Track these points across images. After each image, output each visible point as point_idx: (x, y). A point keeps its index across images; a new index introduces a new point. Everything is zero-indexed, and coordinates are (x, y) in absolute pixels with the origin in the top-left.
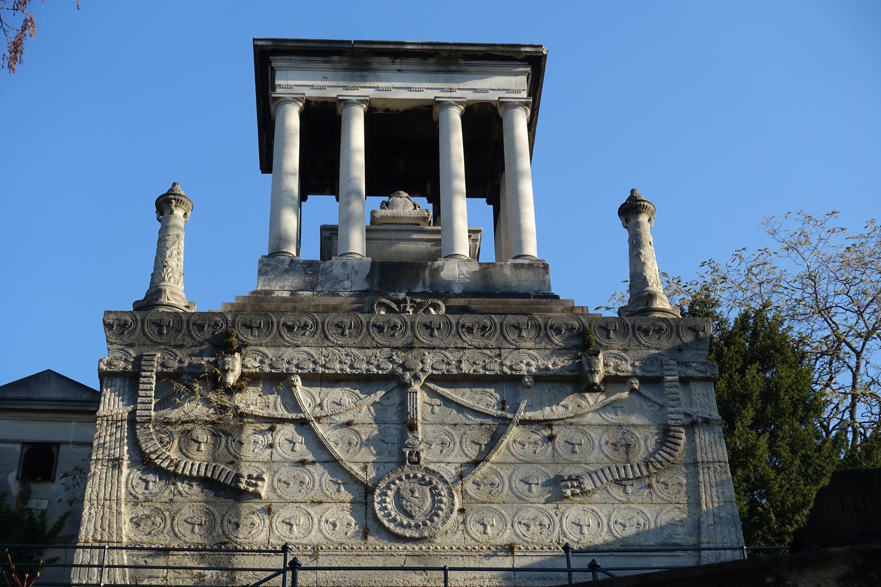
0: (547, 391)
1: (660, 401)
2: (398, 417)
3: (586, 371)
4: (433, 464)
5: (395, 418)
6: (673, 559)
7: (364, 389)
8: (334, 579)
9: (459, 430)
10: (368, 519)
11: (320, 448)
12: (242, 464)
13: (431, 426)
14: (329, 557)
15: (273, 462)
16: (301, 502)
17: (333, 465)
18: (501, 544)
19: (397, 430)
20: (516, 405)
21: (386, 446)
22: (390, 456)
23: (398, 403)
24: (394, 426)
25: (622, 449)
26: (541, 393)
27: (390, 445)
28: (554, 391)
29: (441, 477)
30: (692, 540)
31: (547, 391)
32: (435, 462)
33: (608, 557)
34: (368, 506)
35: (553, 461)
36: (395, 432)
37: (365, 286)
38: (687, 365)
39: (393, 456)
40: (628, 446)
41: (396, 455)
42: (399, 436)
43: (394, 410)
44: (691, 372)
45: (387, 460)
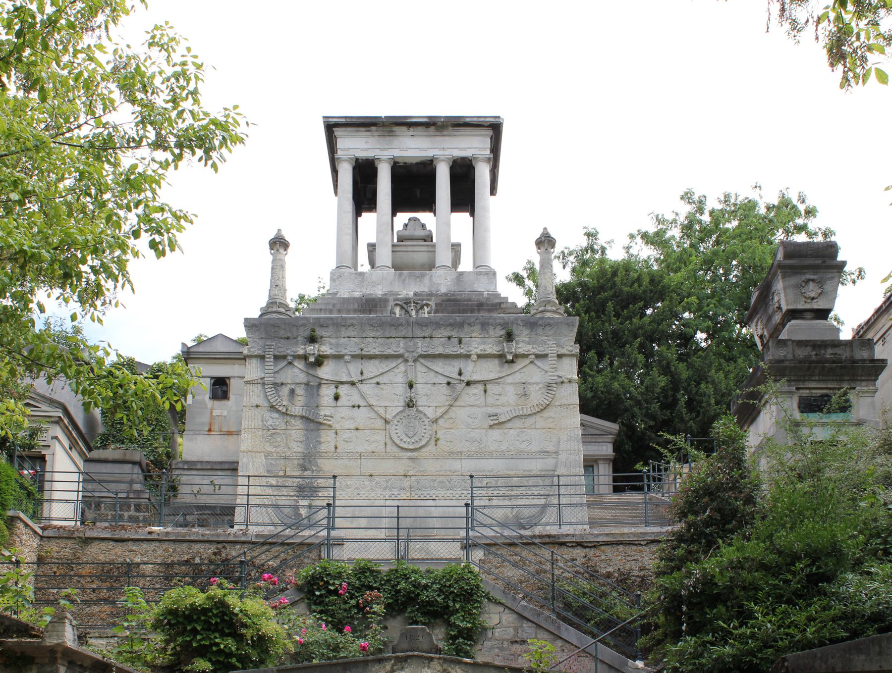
17: (369, 408)
29: (425, 415)
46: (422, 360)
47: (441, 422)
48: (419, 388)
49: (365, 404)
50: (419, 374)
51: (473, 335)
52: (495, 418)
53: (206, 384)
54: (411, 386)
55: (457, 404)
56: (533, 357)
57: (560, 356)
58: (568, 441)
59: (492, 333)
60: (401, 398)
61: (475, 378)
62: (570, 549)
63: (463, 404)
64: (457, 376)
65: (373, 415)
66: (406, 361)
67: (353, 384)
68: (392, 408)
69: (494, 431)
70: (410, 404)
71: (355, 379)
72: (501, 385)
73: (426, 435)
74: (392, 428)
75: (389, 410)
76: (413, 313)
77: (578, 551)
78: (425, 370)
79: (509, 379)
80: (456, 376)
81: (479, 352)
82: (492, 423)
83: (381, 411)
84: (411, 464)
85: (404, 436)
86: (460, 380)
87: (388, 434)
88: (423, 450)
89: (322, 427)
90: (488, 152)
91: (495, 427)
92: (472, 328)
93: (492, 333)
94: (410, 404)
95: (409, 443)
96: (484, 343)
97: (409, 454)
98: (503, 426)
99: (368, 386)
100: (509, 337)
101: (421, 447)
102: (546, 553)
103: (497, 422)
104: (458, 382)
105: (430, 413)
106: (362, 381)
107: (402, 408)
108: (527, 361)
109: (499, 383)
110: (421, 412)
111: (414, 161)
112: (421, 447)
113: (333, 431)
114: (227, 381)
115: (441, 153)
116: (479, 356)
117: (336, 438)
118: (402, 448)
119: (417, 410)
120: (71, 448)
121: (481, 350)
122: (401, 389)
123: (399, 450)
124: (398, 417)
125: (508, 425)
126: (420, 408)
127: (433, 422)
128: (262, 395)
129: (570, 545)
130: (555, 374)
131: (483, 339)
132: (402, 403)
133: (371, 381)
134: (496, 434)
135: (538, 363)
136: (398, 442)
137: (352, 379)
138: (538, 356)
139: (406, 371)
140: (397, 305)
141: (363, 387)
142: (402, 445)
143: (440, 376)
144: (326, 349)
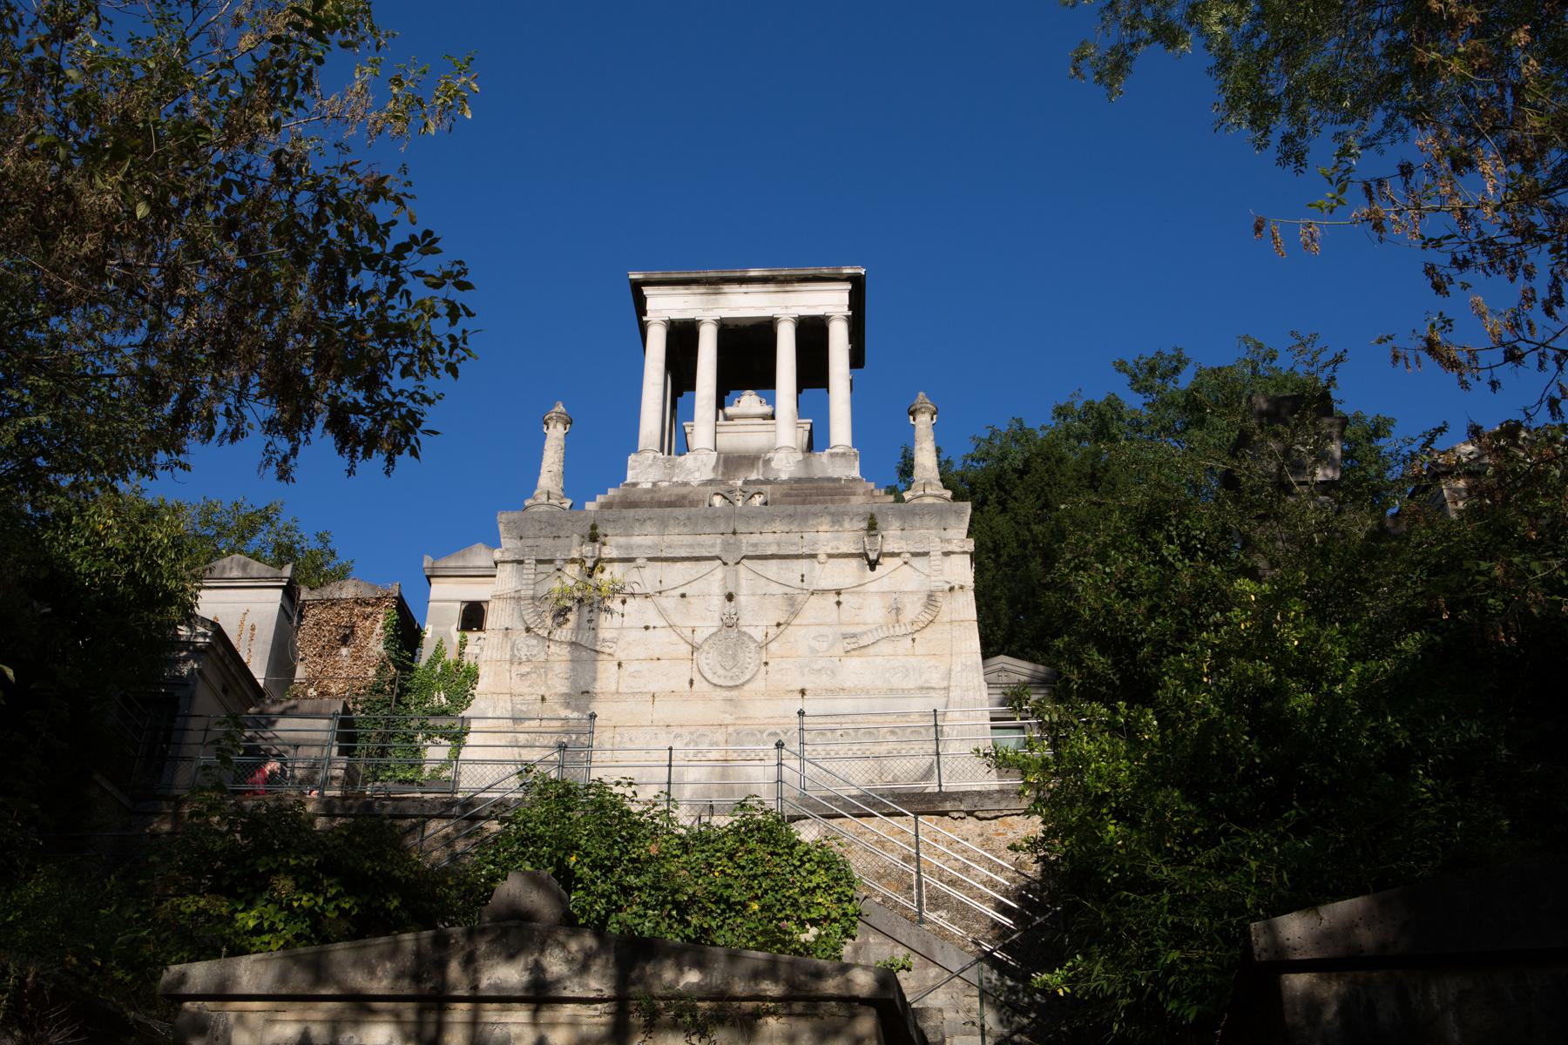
1: (927, 572)
18: (602, 737)
25: (894, 612)
29: (751, 637)
30: (945, 684)
37: (711, 476)
38: (949, 541)
40: (898, 609)
44: (950, 548)
46: (744, 561)
47: (773, 646)
48: (742, 599)
49: (664, 623)
50: (743, 582)
51: (821, 529)
52: (853, 640)
53: (456, 611)
54: (730, 597)
55: (796, 622)
56: (908, 555)
57: (947, 554)
58: (963, 670)
59: (847, 525)
60: (717, 615)
61: (824, 585)
62: (957, 823)
63: (804, 622)
64: (800, 584)
65: (675, 638)
66: (725, 564)
67: (647, 596)
70: (730, 623)
71: (649, 590)
73: (751, 667)
74: (701, 658)
76: (740, 504)
77: (971, 826)
78: (752, 575)
79: (872, 587)
80: (797, 583)
81: (829, 551)
88: (746, 688)
89: (601, 657)
90: (846, 308)
92: (819, 520)
93: (847, 525)
94: (730, 623)
96: (838, 539)
97: (726, 694)
100: (872, 527)
101: (743, 685)
102: (904, 824)
103: (856, 645)
105: (758, 635)
107: (715, 630)
108: (897, 561)
109: (859, 593)
110: (745, 633)
111: (748, 324)
112: (743, 685)
113: (616, 663)
114: (485, 606)
115: (784, 311)
116: (830, 556)
120: (225, 691)
122: (718, 601)
125: (872, 650)
126: (744, 629)
128: (516, 615)
129: (955, 815)
130: (941, 578)
133: (672, 592)
134: (854, 663)
135: (916, 562)
136: (709, 677)
138: (915, 555)
139: (724, 578)
140: (717, 494)
141: (663, 601)
143: (773, 584)
144: (608, 552)
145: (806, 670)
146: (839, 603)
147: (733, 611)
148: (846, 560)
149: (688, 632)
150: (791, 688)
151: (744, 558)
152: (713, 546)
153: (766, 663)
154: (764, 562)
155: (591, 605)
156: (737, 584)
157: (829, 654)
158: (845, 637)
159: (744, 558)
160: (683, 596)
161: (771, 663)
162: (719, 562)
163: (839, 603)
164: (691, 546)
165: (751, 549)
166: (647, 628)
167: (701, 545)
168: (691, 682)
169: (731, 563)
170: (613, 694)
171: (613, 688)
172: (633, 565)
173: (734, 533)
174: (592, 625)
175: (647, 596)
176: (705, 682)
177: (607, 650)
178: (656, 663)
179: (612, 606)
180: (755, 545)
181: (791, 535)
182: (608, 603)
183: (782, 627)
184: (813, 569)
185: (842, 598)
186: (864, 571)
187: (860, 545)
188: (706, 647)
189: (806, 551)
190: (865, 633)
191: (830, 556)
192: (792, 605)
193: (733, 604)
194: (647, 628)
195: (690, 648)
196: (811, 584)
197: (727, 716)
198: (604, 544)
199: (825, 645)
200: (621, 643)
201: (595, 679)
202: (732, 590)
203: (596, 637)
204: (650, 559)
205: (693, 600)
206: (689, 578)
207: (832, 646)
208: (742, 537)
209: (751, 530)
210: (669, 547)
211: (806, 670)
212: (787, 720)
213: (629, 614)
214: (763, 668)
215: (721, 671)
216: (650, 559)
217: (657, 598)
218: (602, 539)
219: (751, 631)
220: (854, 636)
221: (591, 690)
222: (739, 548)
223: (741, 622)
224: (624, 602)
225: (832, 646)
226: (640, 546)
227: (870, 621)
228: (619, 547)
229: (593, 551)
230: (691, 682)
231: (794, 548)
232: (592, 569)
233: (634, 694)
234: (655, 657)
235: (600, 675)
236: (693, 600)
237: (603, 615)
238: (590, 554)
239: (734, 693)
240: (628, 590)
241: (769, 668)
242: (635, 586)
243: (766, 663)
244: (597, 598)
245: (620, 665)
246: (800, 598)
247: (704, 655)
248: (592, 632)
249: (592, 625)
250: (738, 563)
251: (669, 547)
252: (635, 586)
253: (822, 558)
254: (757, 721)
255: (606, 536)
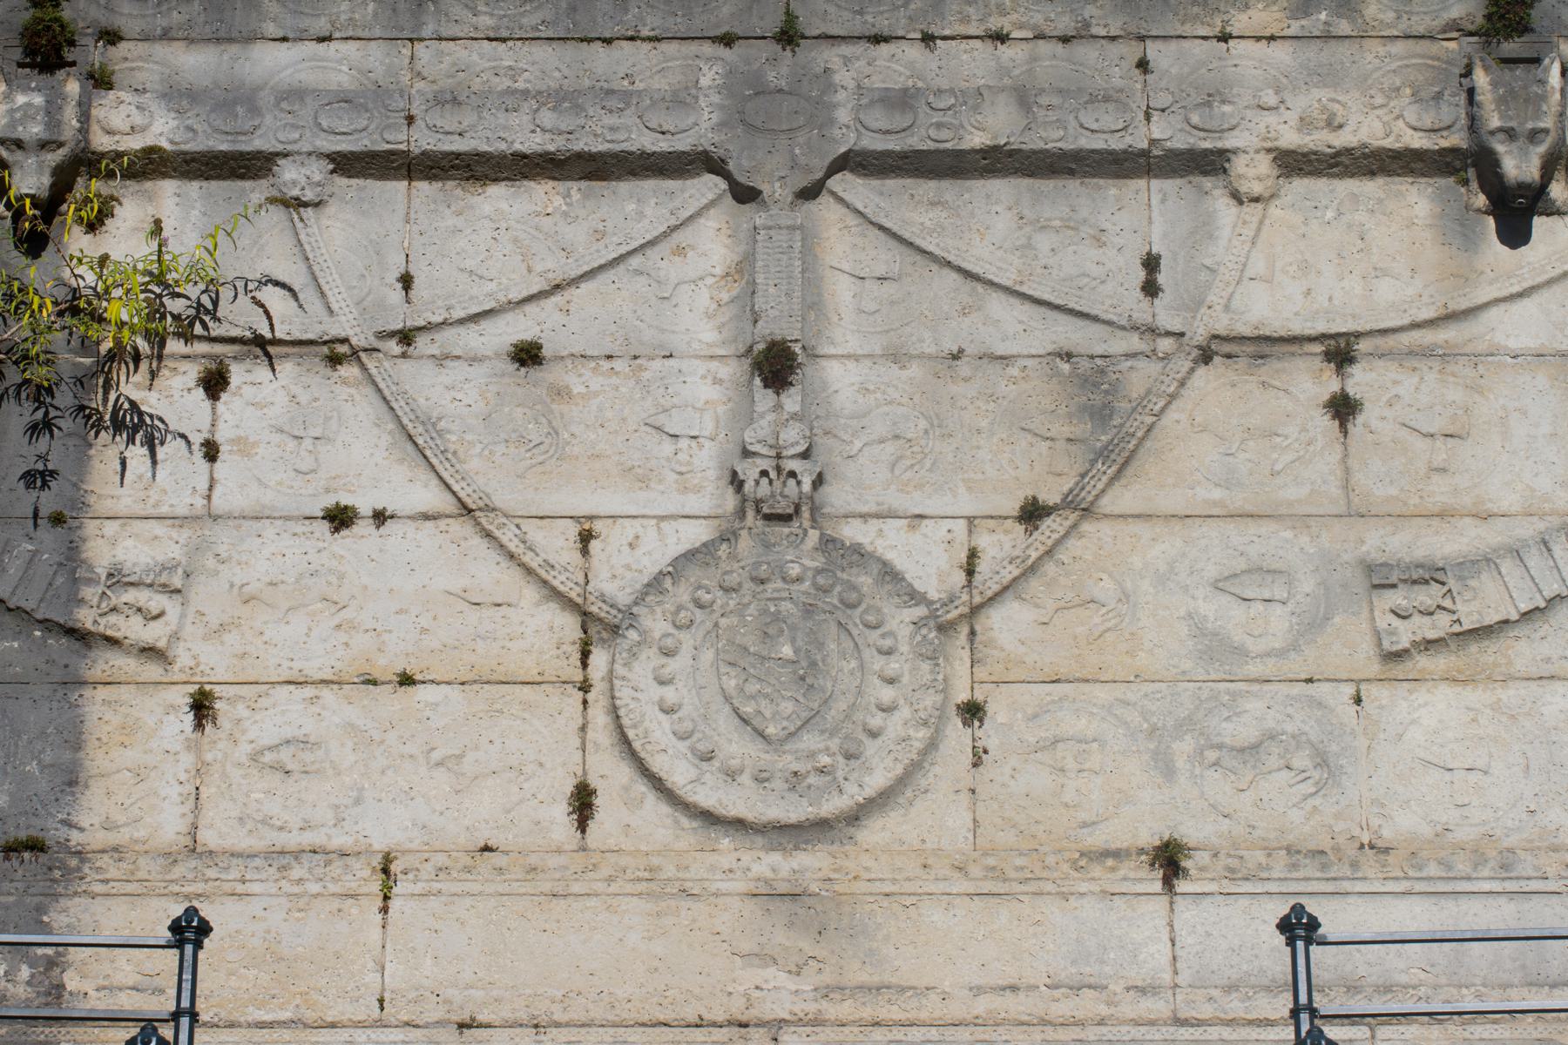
0: (1330, 214)
2: (720, 329)
3: (1492, 133)
4: (857, 522)
5: (707, 334)
6: (1449, 904)
7: (582, 213)
8: (450, 992)
9: (966, 380)
10: (589, 746)
11: (401, 461)
12: (91, 527)
13: (851, 365)
14: (433, 903)
15: (216, 518)
16: (323, 682)
19: (717, 381)
20: (1204, 276)
21: (668, 447)
22: (685, 490)
23: (718, 271)
24: (701, 367)
26: (1306, 222)
27: (684, 443)
28: (1361, 216)
29: (889, 574)
31: (1330, 214)
32: (864, 517)
33: (1555, 898)
34: (590, 697)
35: (1342, 509)
36: (707, 391)
39: (698, 489)
41: (710, 488)
42: (721, 409)
43: (704, 299)
45: (671, 509)
46: (847, 184)
50: (841, 292)
51: (1240, 22)
52: (1428, 596)
55: (1121, 499)
60: (707, 461)
64: (1134, 304)
65: (489, 572)
66: (745, 195)
67: (335, 353)
68: (630, 529)
69: (1421, 695)
71: (348, 325)
72: (1462, 368)
73: (895, 725)
75: (610, 551)
78: (884, 257)
81: (1290, 139)
82: (1405, 634)
83: (556, 545)
84: (781, 937)
85: (724, 721)
86: (1152, 331)
87: (599, 717)
88: (874, 832)
89: (106, 663)
91: (1423, 661)
95: (761, 779)
96: (1326, 76)
98: (1486, 654)
99: (457, 371)
101: (855, 817)
103: (1440, 626)
104: (1135, 342)
106: (406, 337)
107: (696, 534)
109: (1446, 356)
112: (855, 817)
113: (181, 698)
116: (1293, 163)
117: (194, 747)
118: (709, 818)
119: (828, 543)
121: (1305, 123)
123: (687, 834)
124: (682, 593)
125: (1523, 651)
126: (852, 532)
127: (944, 628)
131: (1312, 52)
132: (713, 498)
136: (679, 774)
137: (335, 331)
139: (744, 269)
142: (705, 797)
143: (998, 305)
145: (1184, 747)
146: (1343, 408)
147: (793, 437)
148: (1371, 188)
149: (556, 545)
150: (1097, 839)
151: (842, 164)
152: (681, 100)
153: (972, 712)
154: (948, 189)
155: (41, 393)
156: (814, 305)
157: (1297, 666)
158: (1379, 577)
159: (842, 164)
160: (527, 355)
161: (998, 711)
162: (709, 186)
163: (1343, 408)
164: (562, 99)
165: (878, 119)
166: (340, 518)
167: (614, 97)
168: (583, 802)
169: (776, 190)
170: (170, 858)
171: (169, 825)
172: (256, 191)
173: (788, 36)
174: (49, 501)
175: (335, 353)
176: (654, 807)
177: (133, 629)
178: (391, 701)
179: (151, 403)
180: (901, 100)
181: (1087, 53)
182: (131, 386)
183: (1051, 527)
184: (1204, 229)
185: (1360, 380)
186: (1469, 241)
187: (1453, 110)
188: (656, 623)
189: (1168, 132)
190: (1487, 561)
191: (1293, 163)
192: (1101, 414)
193: (791, 401)
194: (340, 518)
195: (569, 626)
196: (1196, 304)
197: (774, 976)
198: (101, 81)
199: (1279, 623)
200: (209, 595)
201: (71, 780)
202: (778, 324)
203: (72, 558)
204: (346, 164)
205: (576, 380)
206: (555, 266)
207: (1312, 625)
208: (831, 56)
209: (883, 25)
210: (449, 100)
211: (1184, 747)
212: (1088, 1005)
213: (244, 446)
214: (957, 735)
215: (737, 747)
216: (346, 164)
217: (390, 368)
218: (93, 54)
219: (889, 542)
220: (1429, 574)
221: (54, 833)
222: (820, 114)
223: (836, 496)
224: (215, 383)
225: (1312, 625)
226: (294, 95)
227: (1509, 501)
228: (178, 95)
229: (52, 111)
230: (583, 802)
231: (1109, 118)
232: (50, 207)
233: (281, 857)
234: (388, 664)
235: (96, 759)
236: (576, 380)
237: (107, 450)
238: (34, 130)
239: (811, 862)
240: (238, 317)
241: (989, 733)
242: (273, 297)
243: (972, 712)
244: (72, 361)
245: (202, 707)
246: (1140, 377)
247: (647, 662)
248: (47, 534)
249: (49, 501)
250: (810, 193)
251: (449, 100)
252: (273, 297)
253: (1253, 171)
254: (931, 1008)
255: (111, 37)
